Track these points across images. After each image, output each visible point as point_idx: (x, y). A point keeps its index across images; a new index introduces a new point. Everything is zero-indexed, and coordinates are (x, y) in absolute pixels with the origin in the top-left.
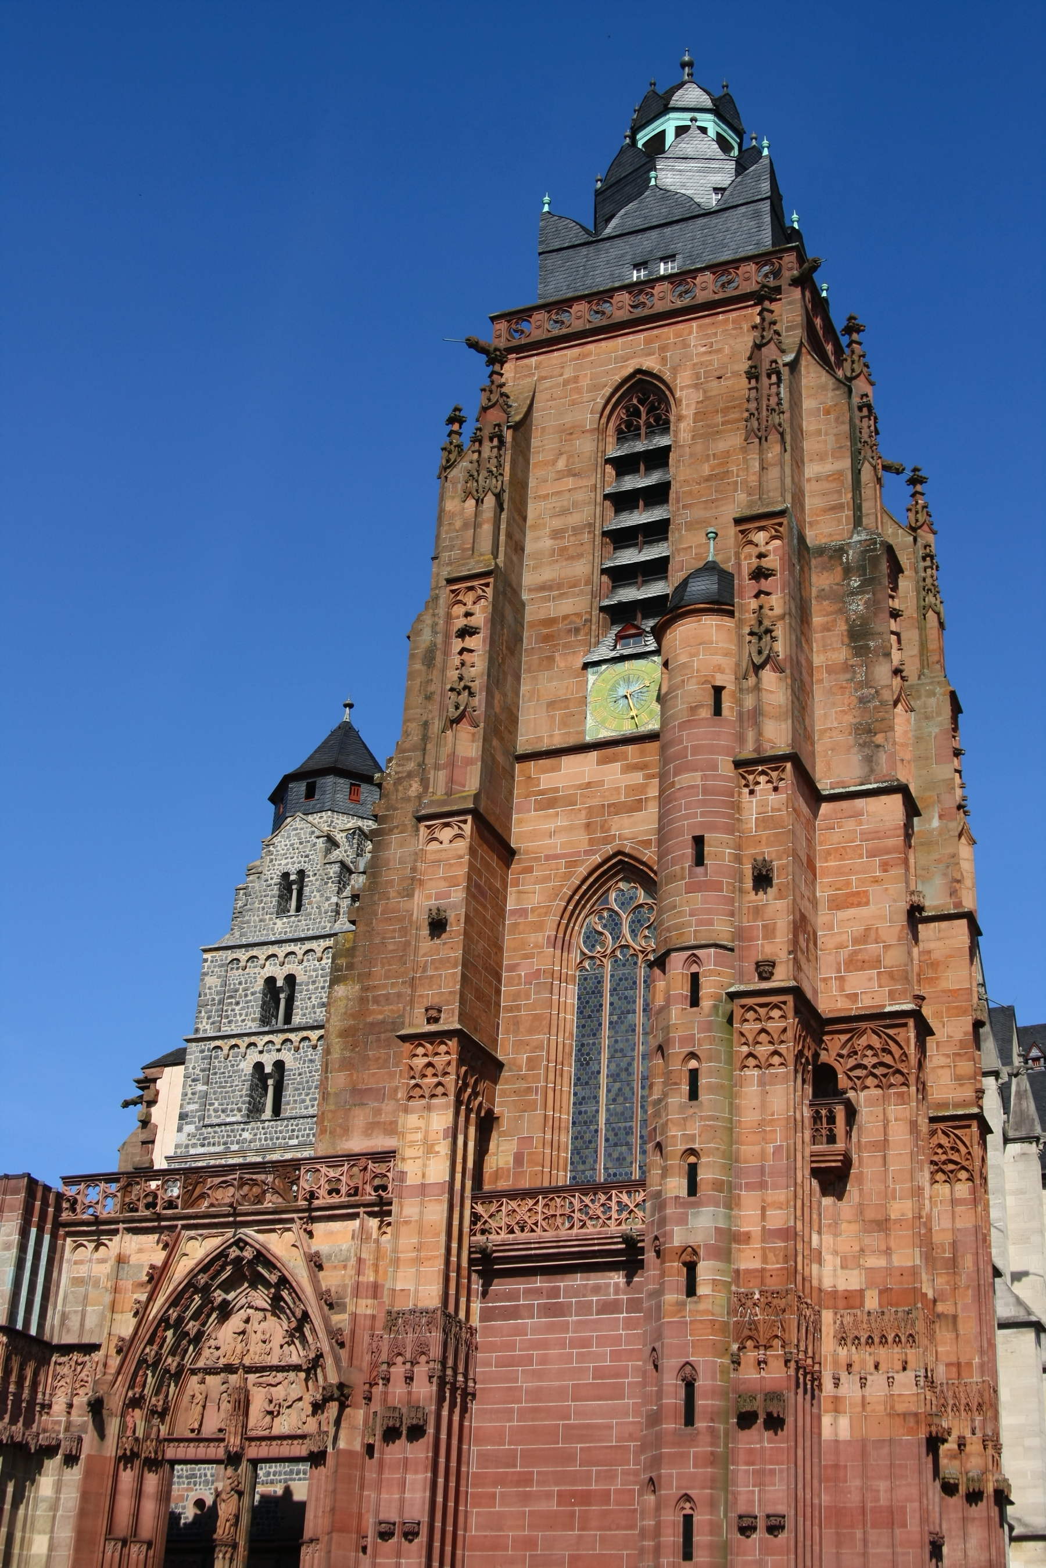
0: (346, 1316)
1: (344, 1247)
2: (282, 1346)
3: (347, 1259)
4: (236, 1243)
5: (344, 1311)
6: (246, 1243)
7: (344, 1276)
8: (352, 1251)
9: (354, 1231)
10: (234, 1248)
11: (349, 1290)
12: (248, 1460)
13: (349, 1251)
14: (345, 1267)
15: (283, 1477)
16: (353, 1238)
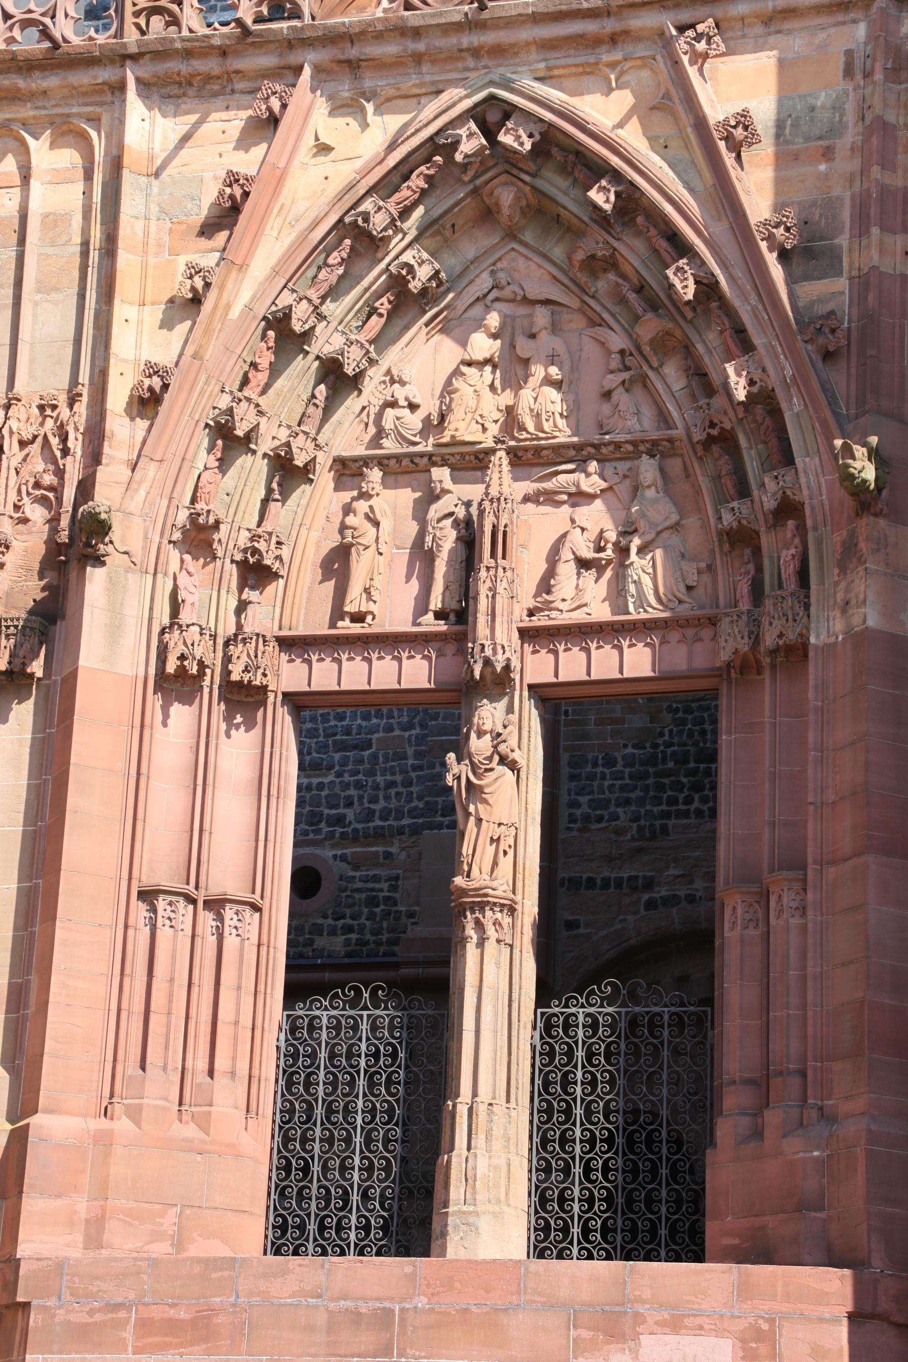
0: (841, 284)
1: (822, 99)
2: (607, 395)
3: (836, 131)
4: (477, 114)
5: (834, 269)
6: (509, 111)
7: (826, 176)
8: (850, 108)
9: (849, 53)
10: (473, 126)
11: (846, 215)
12: (533, 688)
13: (837, 108)
14: (828, 154)
15: (406, 821)
16: (848, 72)
